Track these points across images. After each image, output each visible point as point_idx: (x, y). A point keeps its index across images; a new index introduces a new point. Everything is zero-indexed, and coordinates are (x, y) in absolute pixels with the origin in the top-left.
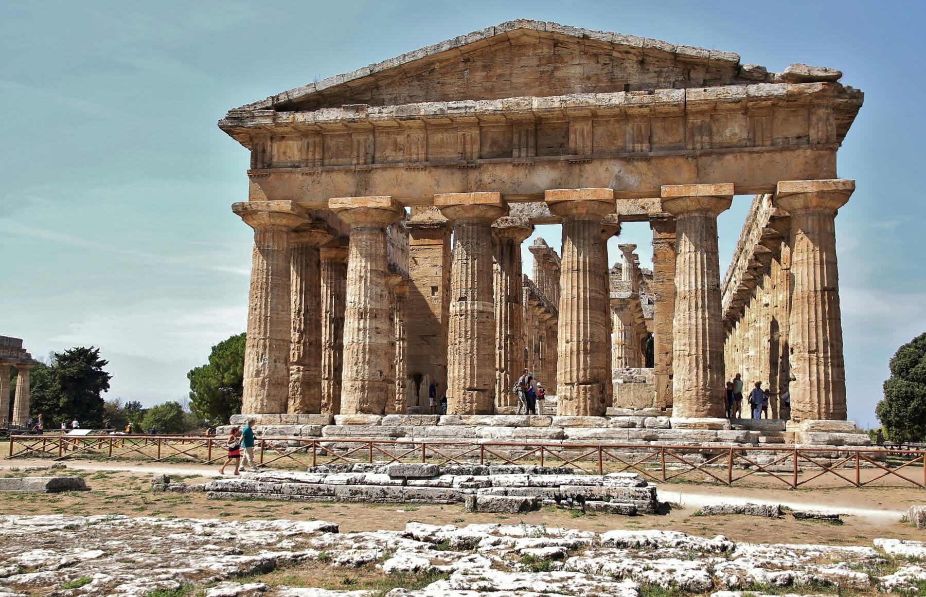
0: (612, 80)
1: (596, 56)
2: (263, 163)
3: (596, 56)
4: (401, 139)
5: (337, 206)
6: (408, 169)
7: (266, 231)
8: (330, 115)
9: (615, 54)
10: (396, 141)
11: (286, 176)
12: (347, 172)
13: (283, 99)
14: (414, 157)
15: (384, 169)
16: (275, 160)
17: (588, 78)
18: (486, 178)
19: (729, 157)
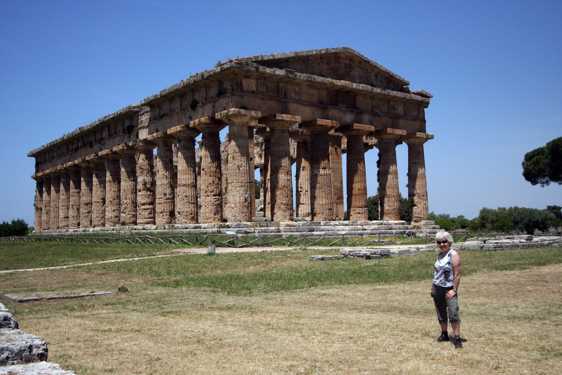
0: (368, 80)
1: (362, 68)
2: (241, 89)
3: (362, 68)
4: (297, 89)
5: (280, 118)
6: (303, 104)
7: (244, 126)
8: (280, 72)
9: (369, 70)
10: (295, 89)
11: (252, 98)
12: (277, 101)
13: (260, 59)
14: (304, 99)
15: (293, 102)
16: (245, 88)
17: (361, 78)
18: (330, 114)
19: (401, 120)
